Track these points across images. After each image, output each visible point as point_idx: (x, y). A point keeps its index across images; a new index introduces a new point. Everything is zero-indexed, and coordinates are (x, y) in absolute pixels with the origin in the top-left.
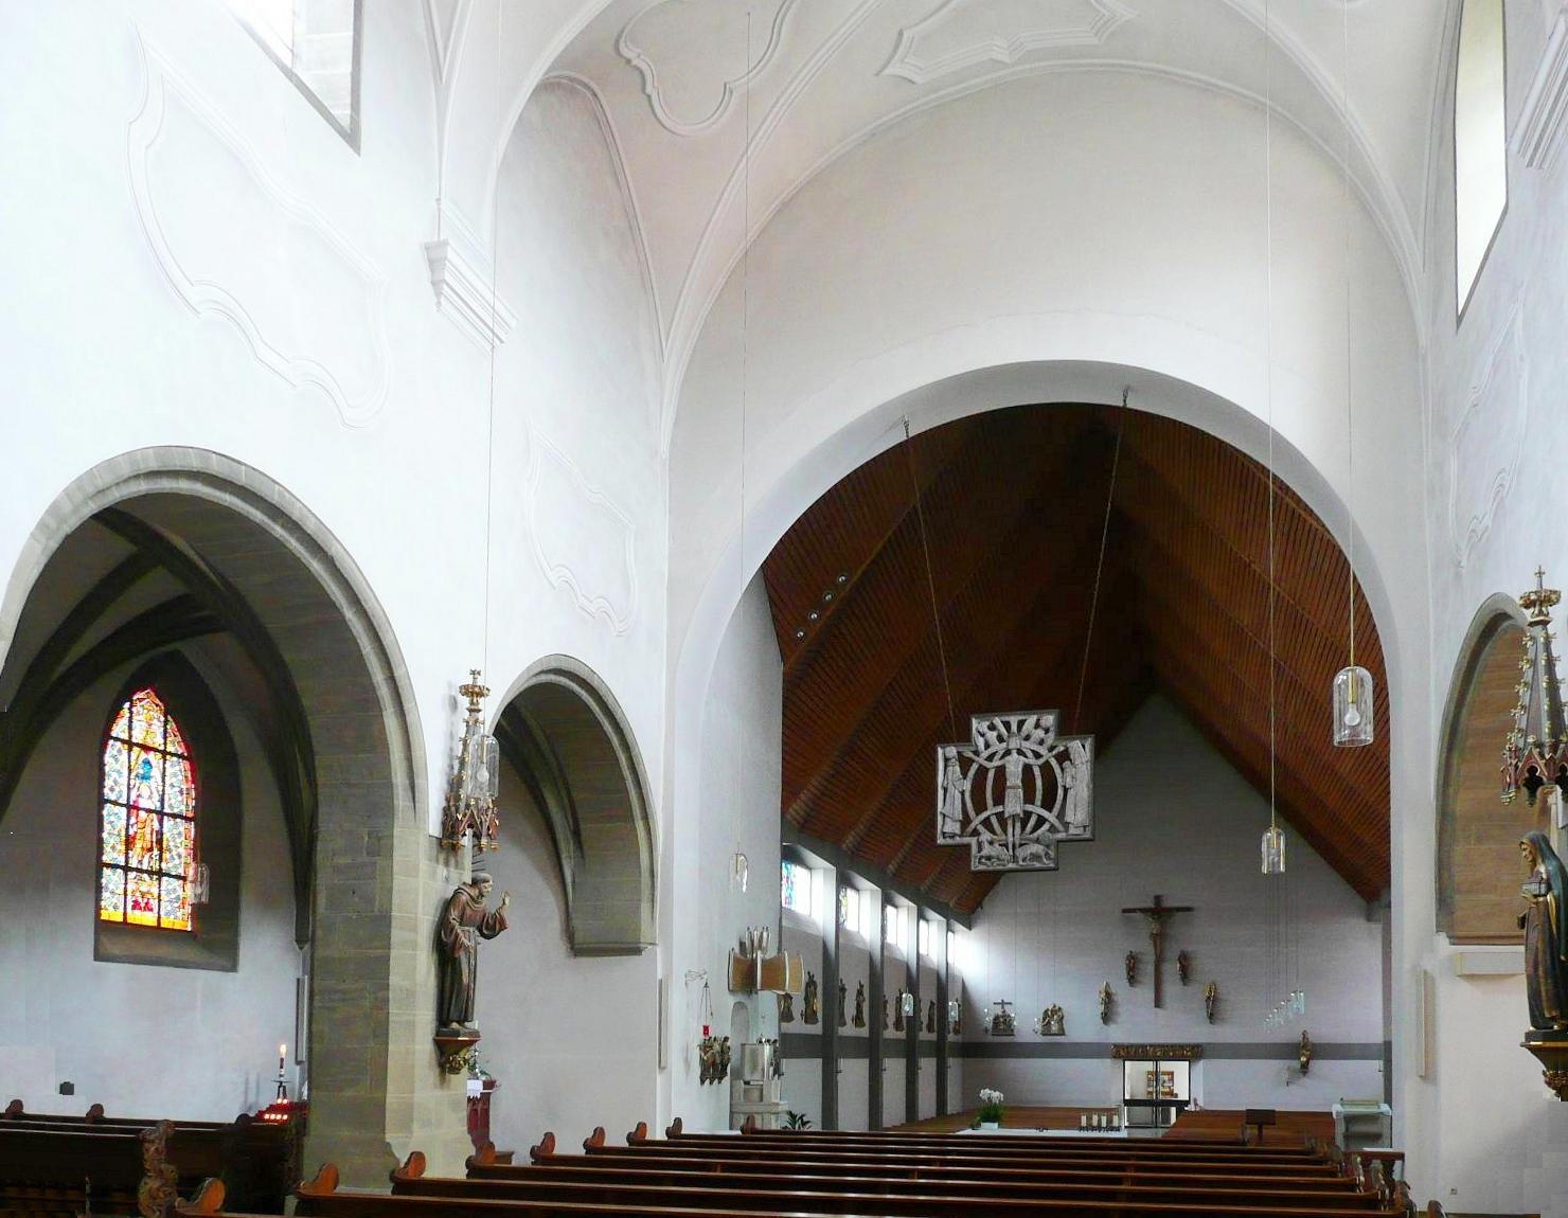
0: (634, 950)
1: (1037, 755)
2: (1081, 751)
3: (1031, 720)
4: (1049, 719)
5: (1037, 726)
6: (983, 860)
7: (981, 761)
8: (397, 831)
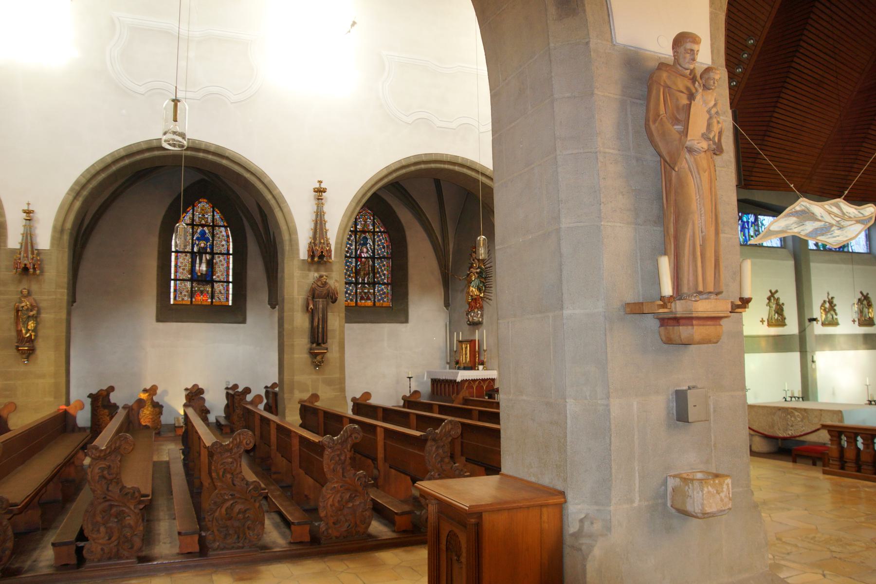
8: (286, 261)
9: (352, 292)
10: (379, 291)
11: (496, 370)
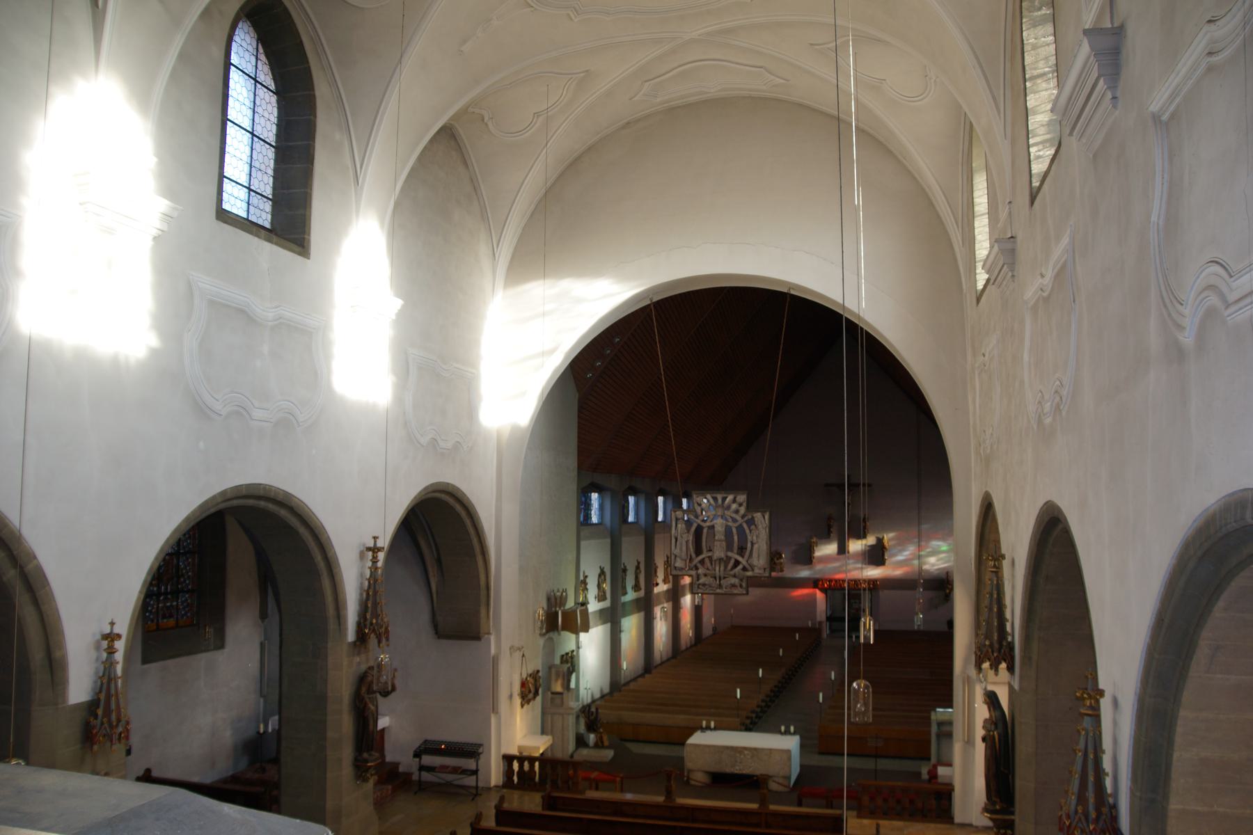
0: (477, 637)
1: (734, 520)
2: (762, 520)
3: (730, 498)
4: (742, 498)
5: (734, 501)
6: (700, 586)
7: (699, 521)
8: (330, 645)
9: (153, 608)
10: (183, 602)
11: (386, 715)
